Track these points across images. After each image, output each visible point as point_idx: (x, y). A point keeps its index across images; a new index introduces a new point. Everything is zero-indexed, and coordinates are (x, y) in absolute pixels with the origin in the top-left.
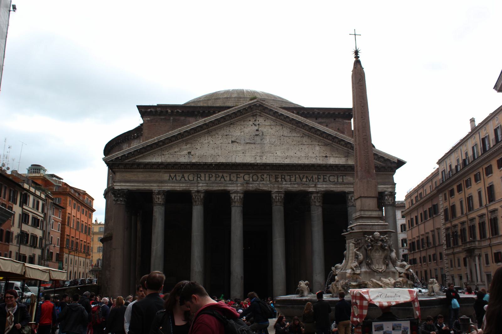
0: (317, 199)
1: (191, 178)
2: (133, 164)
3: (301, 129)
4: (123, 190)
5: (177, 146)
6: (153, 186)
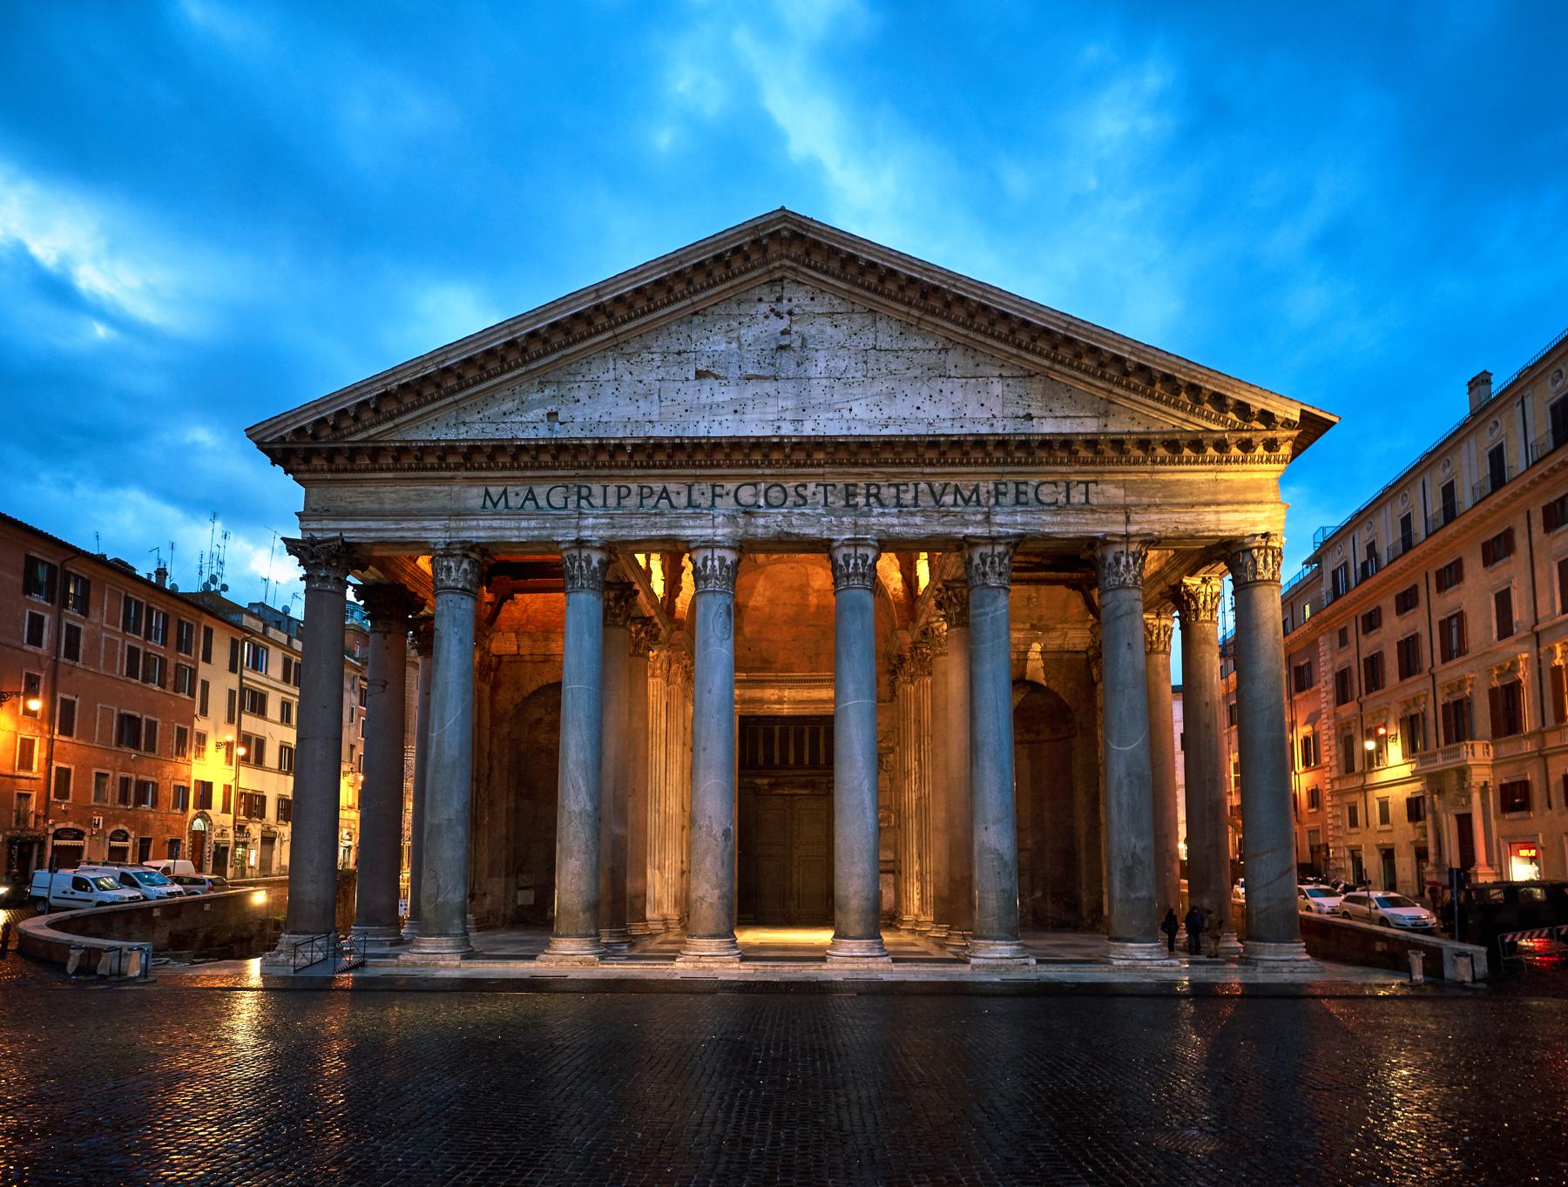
0: (993, 563)
4: (326, 545)
5: (508, 392)
6: (431, 530)
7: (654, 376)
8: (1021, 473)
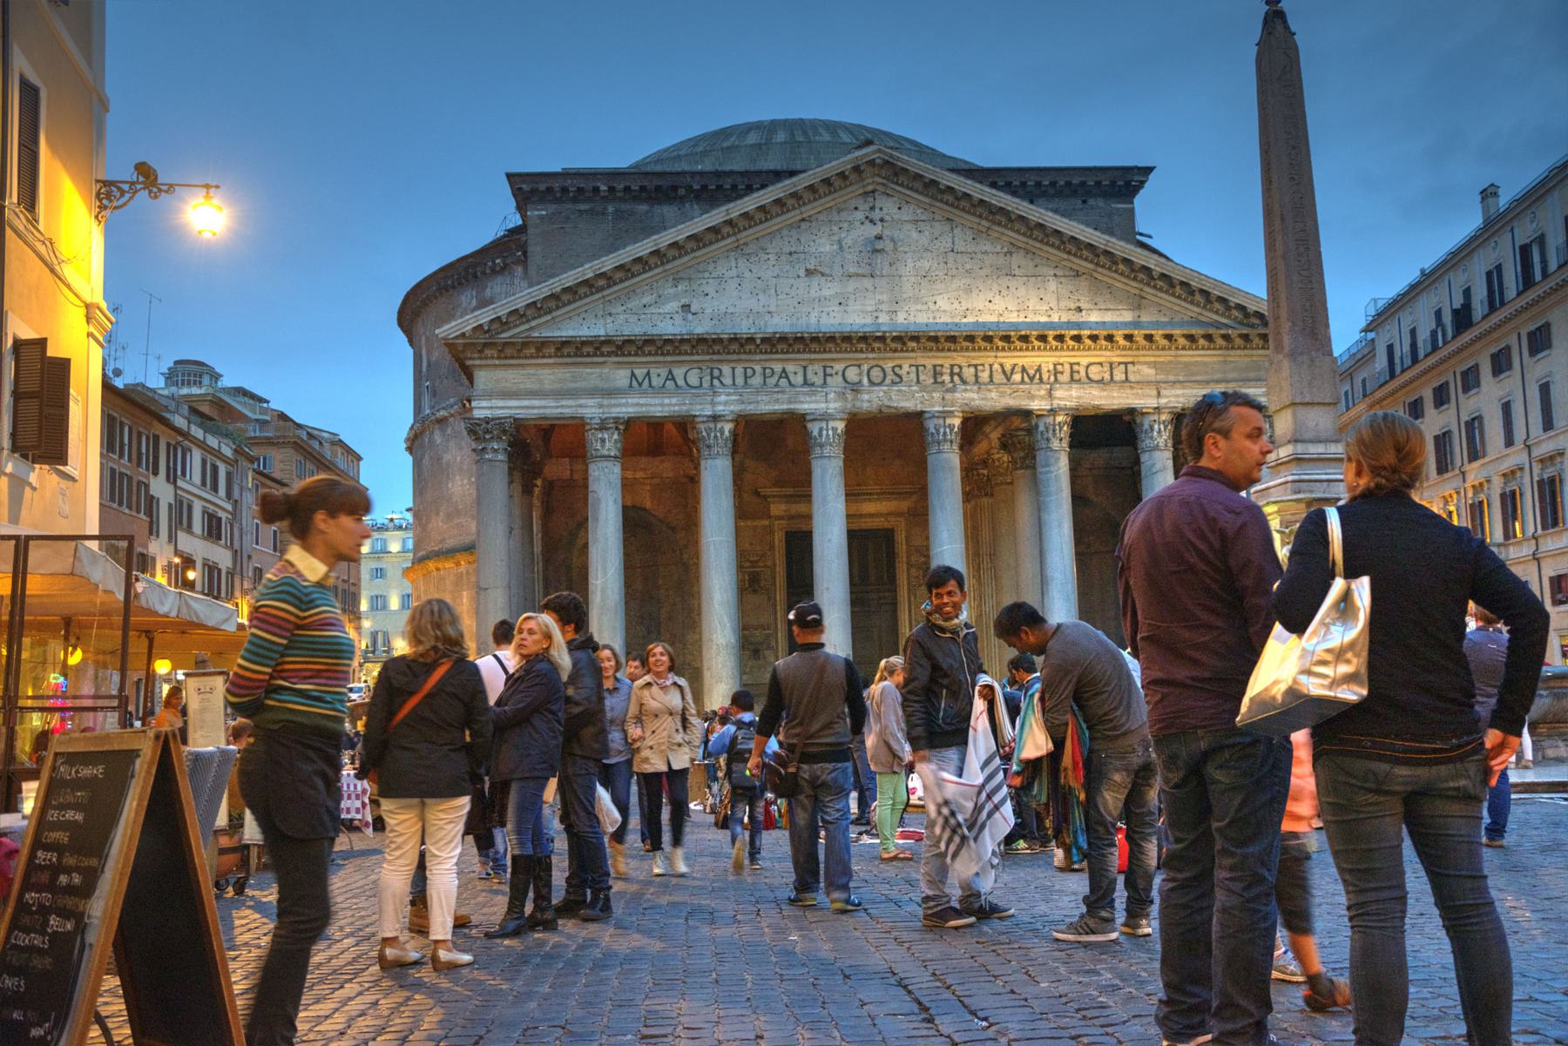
1: (693, 380)
2: (525, 345)
7: (770, 273)
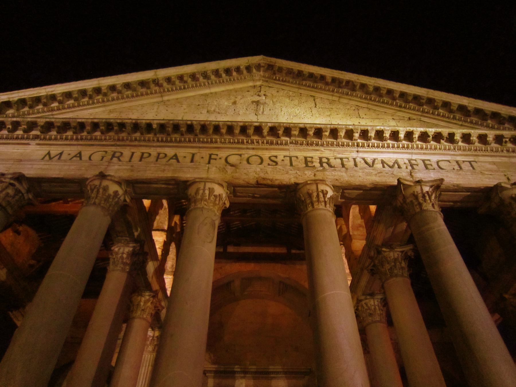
3: (350, 97)
8: (424, 154)
